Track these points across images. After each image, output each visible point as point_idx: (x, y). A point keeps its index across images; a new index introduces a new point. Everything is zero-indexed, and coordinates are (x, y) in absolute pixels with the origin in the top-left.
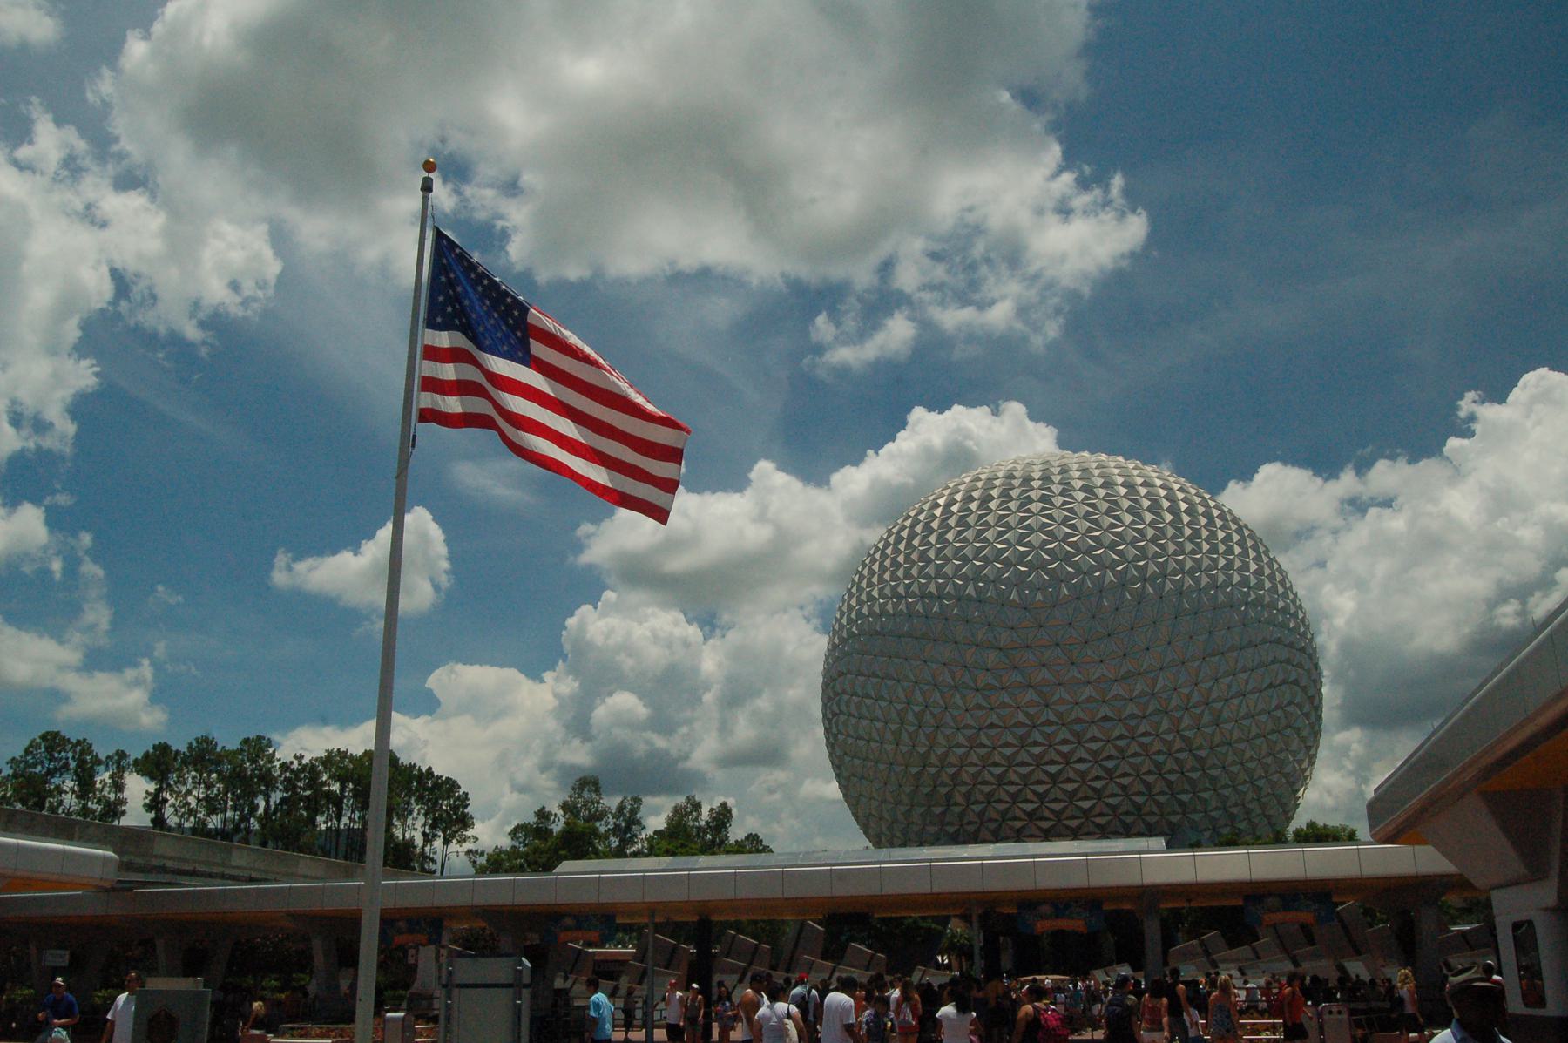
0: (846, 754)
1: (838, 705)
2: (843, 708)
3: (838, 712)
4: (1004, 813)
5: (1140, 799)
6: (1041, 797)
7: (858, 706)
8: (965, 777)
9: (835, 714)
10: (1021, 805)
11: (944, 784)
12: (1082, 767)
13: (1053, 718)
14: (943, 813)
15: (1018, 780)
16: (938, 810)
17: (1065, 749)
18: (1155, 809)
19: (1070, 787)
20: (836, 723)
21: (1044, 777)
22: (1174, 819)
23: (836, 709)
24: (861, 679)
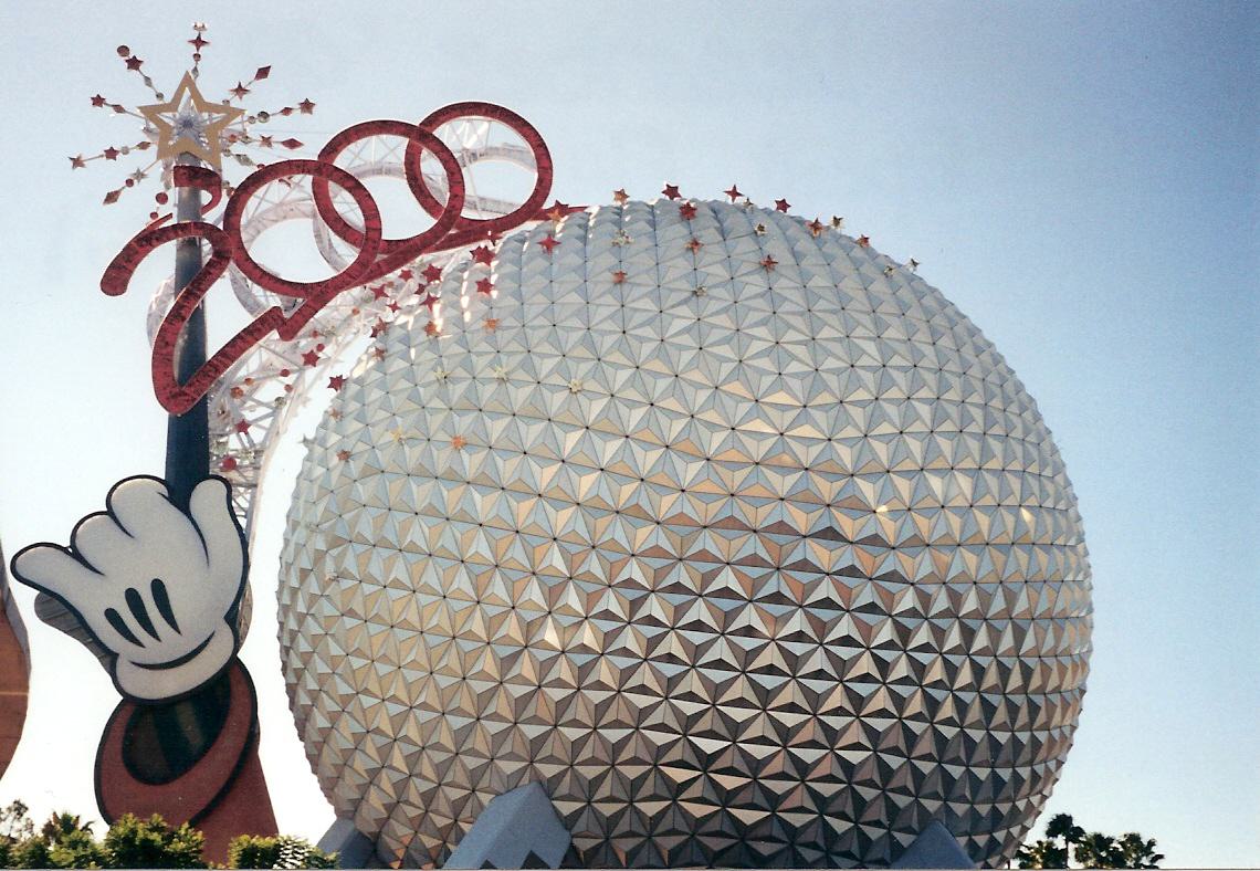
6: (735, 729)
8: (604, 673)
10: (690, 738)
11: (560, 683)
14: (543, 738)
15: (703, 695)
16: (533, 731)
20: (339, 560)
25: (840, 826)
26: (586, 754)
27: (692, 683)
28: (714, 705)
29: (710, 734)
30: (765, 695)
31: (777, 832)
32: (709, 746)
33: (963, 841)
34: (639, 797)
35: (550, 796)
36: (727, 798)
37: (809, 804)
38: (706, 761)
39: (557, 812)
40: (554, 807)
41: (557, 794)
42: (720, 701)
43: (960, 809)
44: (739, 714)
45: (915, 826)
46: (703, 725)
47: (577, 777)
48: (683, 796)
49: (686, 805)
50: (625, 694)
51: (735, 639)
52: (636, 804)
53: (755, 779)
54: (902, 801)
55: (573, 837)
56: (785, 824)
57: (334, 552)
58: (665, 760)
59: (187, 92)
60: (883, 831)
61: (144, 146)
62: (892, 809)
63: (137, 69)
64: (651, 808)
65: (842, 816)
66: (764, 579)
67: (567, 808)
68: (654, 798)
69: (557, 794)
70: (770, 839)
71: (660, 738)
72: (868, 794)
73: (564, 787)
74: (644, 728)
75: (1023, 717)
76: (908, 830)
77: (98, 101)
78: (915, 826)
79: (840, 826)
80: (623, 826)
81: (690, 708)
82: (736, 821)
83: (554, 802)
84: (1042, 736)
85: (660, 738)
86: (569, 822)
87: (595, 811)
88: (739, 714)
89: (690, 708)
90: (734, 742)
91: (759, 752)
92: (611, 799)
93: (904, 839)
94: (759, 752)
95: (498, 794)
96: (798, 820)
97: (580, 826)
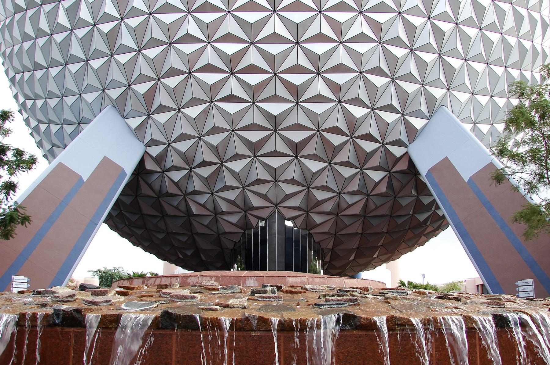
4: (191, 59)
22: (438, 93)
37: (327, 93)
40: (126, 123)
43: (463, 97)
45: (424, 108)
53: (275, 74)
54: (410, 88)
55: (147, 145)
62: (403, 96)
64: (193, 112)
65: (357, 102)
67: (135, 122)
73: (128, 108)
75: (510, 22)
76: (418, 114)
78: (424, 108)
82: (268, 116)
83: (128, 121)
84: (527, 44)
92: (162, 109)
93: (418, 123)
96: (319, 108)
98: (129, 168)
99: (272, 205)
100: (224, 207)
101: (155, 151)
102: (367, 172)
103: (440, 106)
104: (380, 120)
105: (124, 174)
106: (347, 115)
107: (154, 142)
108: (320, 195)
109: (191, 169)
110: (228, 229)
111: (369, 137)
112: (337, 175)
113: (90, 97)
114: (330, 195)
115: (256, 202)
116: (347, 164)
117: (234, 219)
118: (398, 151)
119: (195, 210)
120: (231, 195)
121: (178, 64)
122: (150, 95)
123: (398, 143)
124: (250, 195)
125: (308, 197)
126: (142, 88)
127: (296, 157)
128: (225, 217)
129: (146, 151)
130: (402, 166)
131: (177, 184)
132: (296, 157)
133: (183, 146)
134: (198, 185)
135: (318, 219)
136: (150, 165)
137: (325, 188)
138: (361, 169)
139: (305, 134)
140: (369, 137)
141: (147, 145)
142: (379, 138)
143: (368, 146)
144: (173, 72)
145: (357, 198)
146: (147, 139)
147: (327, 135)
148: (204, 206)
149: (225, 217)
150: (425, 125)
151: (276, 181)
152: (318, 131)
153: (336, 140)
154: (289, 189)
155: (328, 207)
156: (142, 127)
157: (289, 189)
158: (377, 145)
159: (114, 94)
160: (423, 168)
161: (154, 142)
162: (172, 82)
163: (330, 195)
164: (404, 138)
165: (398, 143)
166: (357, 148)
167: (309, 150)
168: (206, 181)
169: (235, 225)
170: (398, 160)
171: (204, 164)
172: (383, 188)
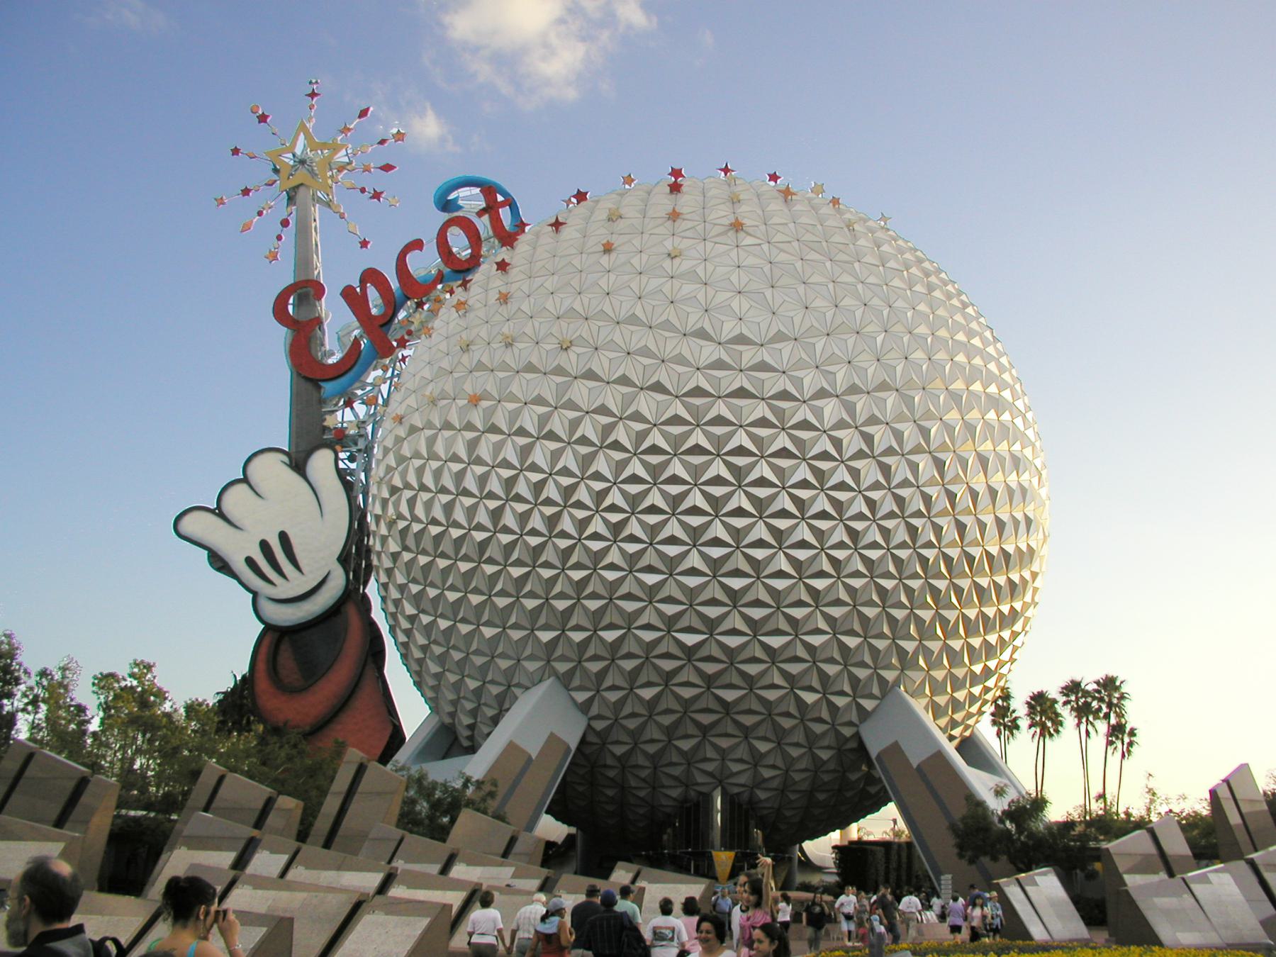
0: (406, 548)
1: (404, 475)
2: (412, 479)
3: (401, 486)
5: (852, 642)
7: (437, 474)
9: (394, 490)
12: (780, 584)
13: (747, 506)
16: (545, 636)
17: (759, 554)
18: (868, 659)
19: (757, 614)
20: (397, 505)
21: (720, 595)
22: (890, 675)
23: (397, 482)
24: (447, 434)
25: (809, 698)
26: (590, 652)
27: (671, 589)
28: (691, 606)
29: (690, 630)
30: (734, 595)
31: (756, 706)
32: (690, 639)
33: (924, 701)
34: (638, 684)
35: (567, 687)
36: (710, 680)
38: (690, 652)
39: (573, 699)
40: (570, 696)
41: (572, 686)
42: (697, 601)
44: (714, 612)
46: (684, 623)
47: (585, 671)
48: (676, 681)
49: (676, 689)
50: (616, 601)
51: (705, 549)
52: (638, 691)
54: (862, 673)
56: (762, 700)
57: (393, 499)
58: (655, 653)
59: (302, 137)
60: (848, 699)
61: (271, 184)
62: (854, 681)
63: (265, 122)
64: (647, 694)
66: (729, 496)
67: (581, 697)
68: (649, 684)
69: (572, 686)
70: (750, 712)
71: (648, 636)
72: (831, 670)
73: (576, 682)
74: (636, 628)
76: (871, 696)
77: (236, 151)
79: (809, 698)
80: (627, 710)
81: (670, 609)
82: (720, 700)
83: (574, 694)
85: (648, 636)
86: (584, 707)
87: (604, 699)
88: (714, 612)
89: (670, 609)
90: (711, 635)
91: (733, 642)
92: (614, 688)
93: (868, 704)
94: (733, 642)
95: (527, 688)
97: (594, 710)
98: (573, 744)
99: (714, 781)
100: (666, 782)
101: (599, 725)
102: (816, 751)
103: (893, 686)
104: (830, 704)
105: (569, 749)
106: (799, 700)
107: (599, 717)
108: (767, 773)
109: (636, 744)
110: (664, 802)
111: (820, 720)
112: (785, 755)
113: (532, 666)
114: (777, 772)
115: (700, 778)
116: (797, 745)
117: (675, 793)
118: (847, 732)
119: (633, 783)
120: (677, 771)
121: (635, 649)
122: (602, 674)
123: (850, 724)
124: (696, 772)
125: (756, 774)
126: (595, 667)
127: (746, 738)
128: (665, 791)
129: (589, 726)
130: (853, 745)
131: (619, 759)
132: (746, 738)
133: (632, 724)
134: (641, 760)
135: (762, 795)
136: (592, 738)
137: (774, 767)
138: (810, 748)
139: (757, 718)
140: (820, 720)
141: (590, 719)
142: (829, 721)
143: (818, 728)
144: (630, 656)
145: (804, 775)
146: (594, 710)
147: (778, 719)
148: (644, 780)
149: (665, 791)
150: (877, 706)
151: (723, 760)
152: (770, 715)
153: (787, 723)
154: (735, 767)
155: (775, 784)
156: (590, 701)
157: (735, 767)
158: (826, 727)
159: (562, 667)
160: (874, 749)
161: (599, 717)
162: (629, 665)
163: (777, 772)
164: (854, 718)
165: (850, 724)
166: (808, 731)
167: (761, 732)
168: (654, 758)
169: (675, 799)
170: (847, 740)
171: (652, 741)
172: (832, 766)
